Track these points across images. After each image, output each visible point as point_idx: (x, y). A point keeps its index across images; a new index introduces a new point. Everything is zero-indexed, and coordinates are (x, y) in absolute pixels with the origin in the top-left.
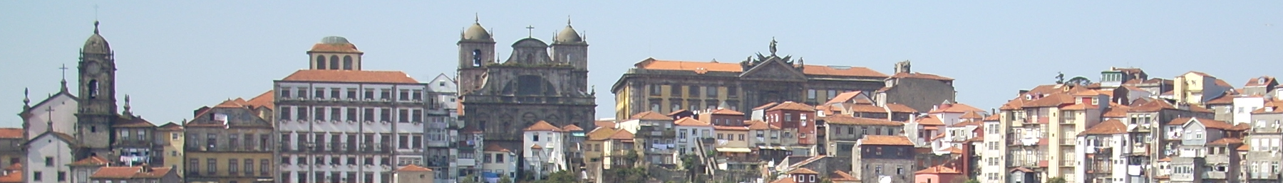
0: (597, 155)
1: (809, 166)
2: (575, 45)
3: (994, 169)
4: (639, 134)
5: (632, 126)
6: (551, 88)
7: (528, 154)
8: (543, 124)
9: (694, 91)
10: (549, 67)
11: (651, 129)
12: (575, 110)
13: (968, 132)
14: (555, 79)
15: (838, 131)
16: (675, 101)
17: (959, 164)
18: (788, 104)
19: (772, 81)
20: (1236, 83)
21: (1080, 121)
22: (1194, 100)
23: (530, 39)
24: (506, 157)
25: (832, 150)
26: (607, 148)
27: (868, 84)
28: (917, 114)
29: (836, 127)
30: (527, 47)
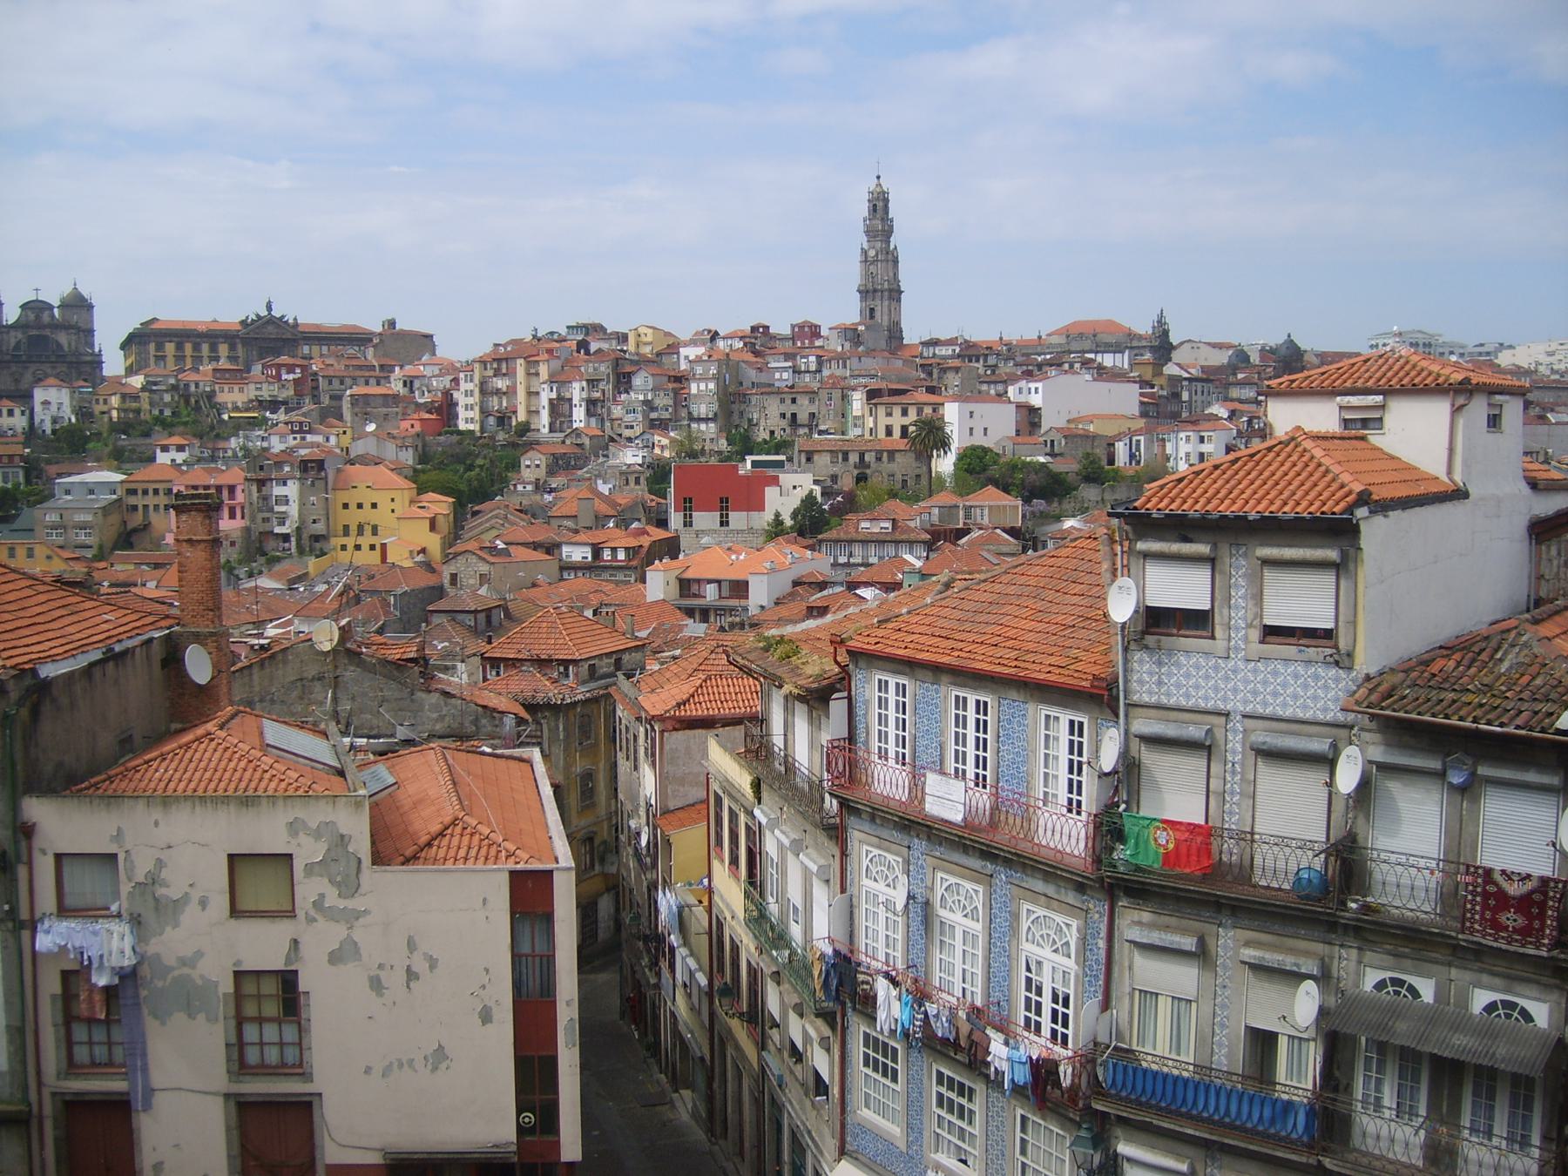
0: (105, 408)
1: (304, 415)
2: (78, 304)
3: (470, 414)
4: (143, 389)
5: (137, 381)
6: (59, 346)
7: (38, 408)
8: (52, 381)
9: (197, 347)
10: (56, 326)
11: (155, 384)
12: (81, 365)
13: (446, 382)
14: (63, 338)
15: (330, 383)
16: (180, 358)
17: (439, 410)
18: (284, 359)
19: (268, 339)
20: (684, 335)
21: (544, 370)
22: (646, 350)
23: (37, 301)
24: (17, 412)
25: (326, 401)
26: (115, 401)
27: (358, 338)
28: (402, 367)
29: (330, 380)
30: (35, 308)
